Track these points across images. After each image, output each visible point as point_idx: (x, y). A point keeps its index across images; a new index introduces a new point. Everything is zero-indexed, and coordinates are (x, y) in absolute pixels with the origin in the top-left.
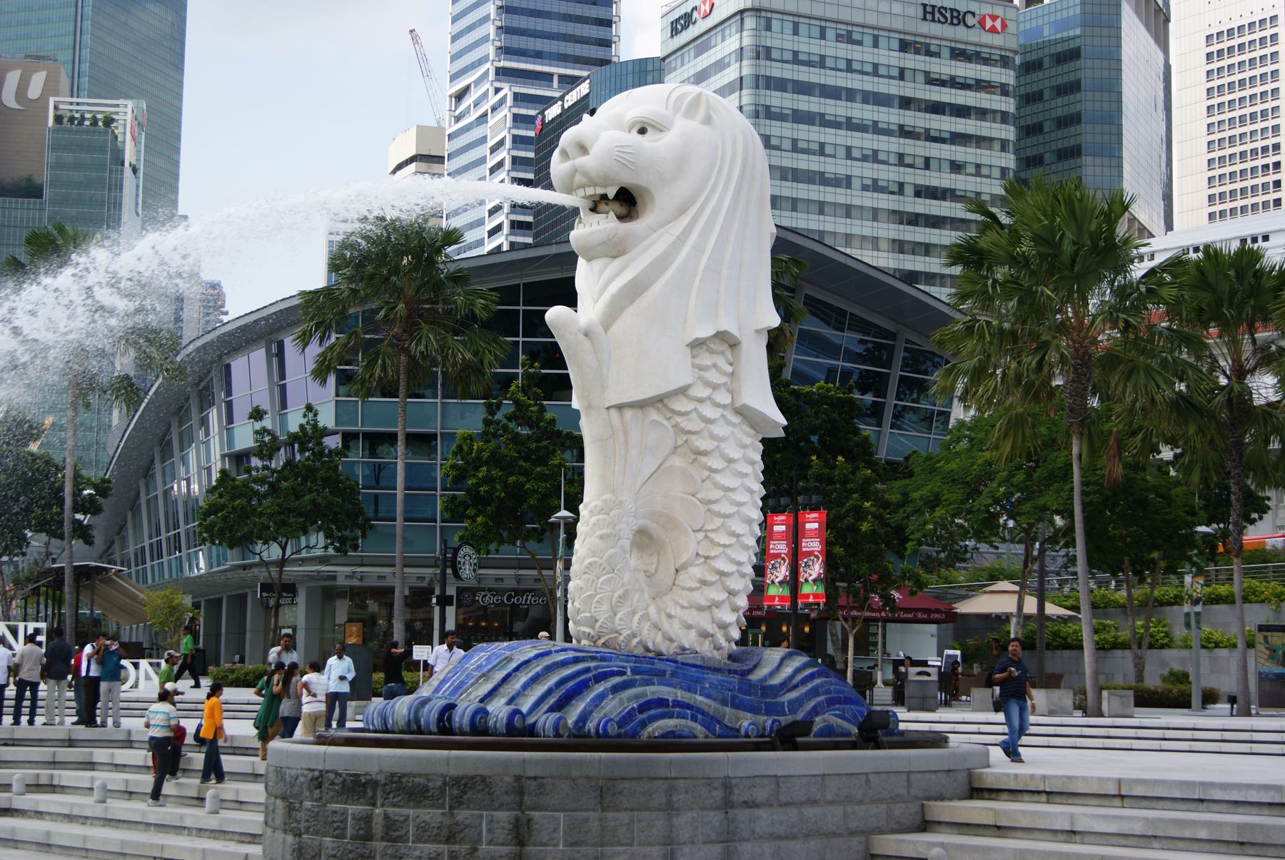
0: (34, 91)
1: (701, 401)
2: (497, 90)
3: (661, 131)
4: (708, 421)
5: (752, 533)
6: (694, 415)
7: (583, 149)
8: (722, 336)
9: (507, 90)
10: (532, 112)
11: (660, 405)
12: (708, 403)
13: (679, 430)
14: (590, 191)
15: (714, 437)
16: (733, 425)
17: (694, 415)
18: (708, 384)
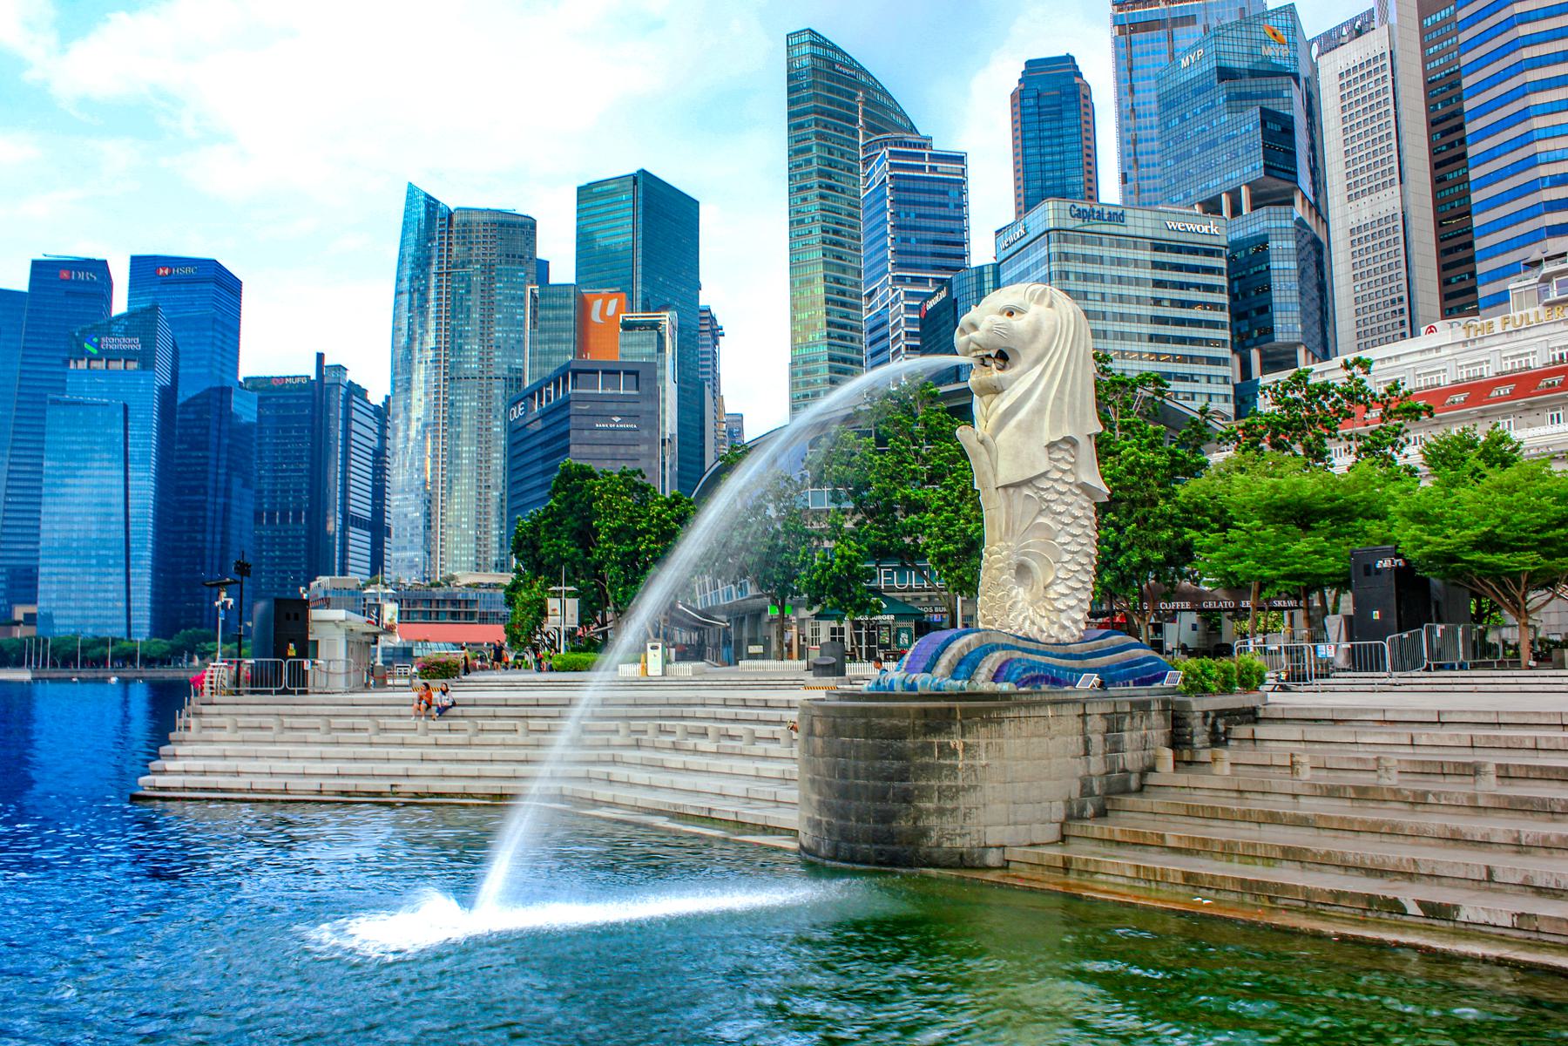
0: (610, 311)
1: (1056, 480)
2: (894, 291)
5: (1092, 563)
7: (974, 327)
8: (1066, 440)
9: (901, 290)
10: (918, 303)
14: (980, 353)
16: (1076, 495)
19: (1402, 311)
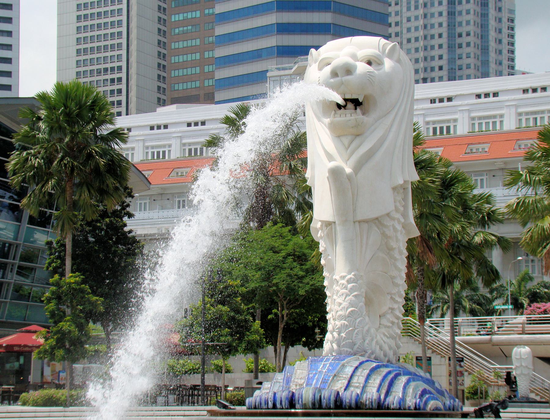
12: (396, 221)
13: (384, 234)
17: (392, 228)
19: (120, 80)
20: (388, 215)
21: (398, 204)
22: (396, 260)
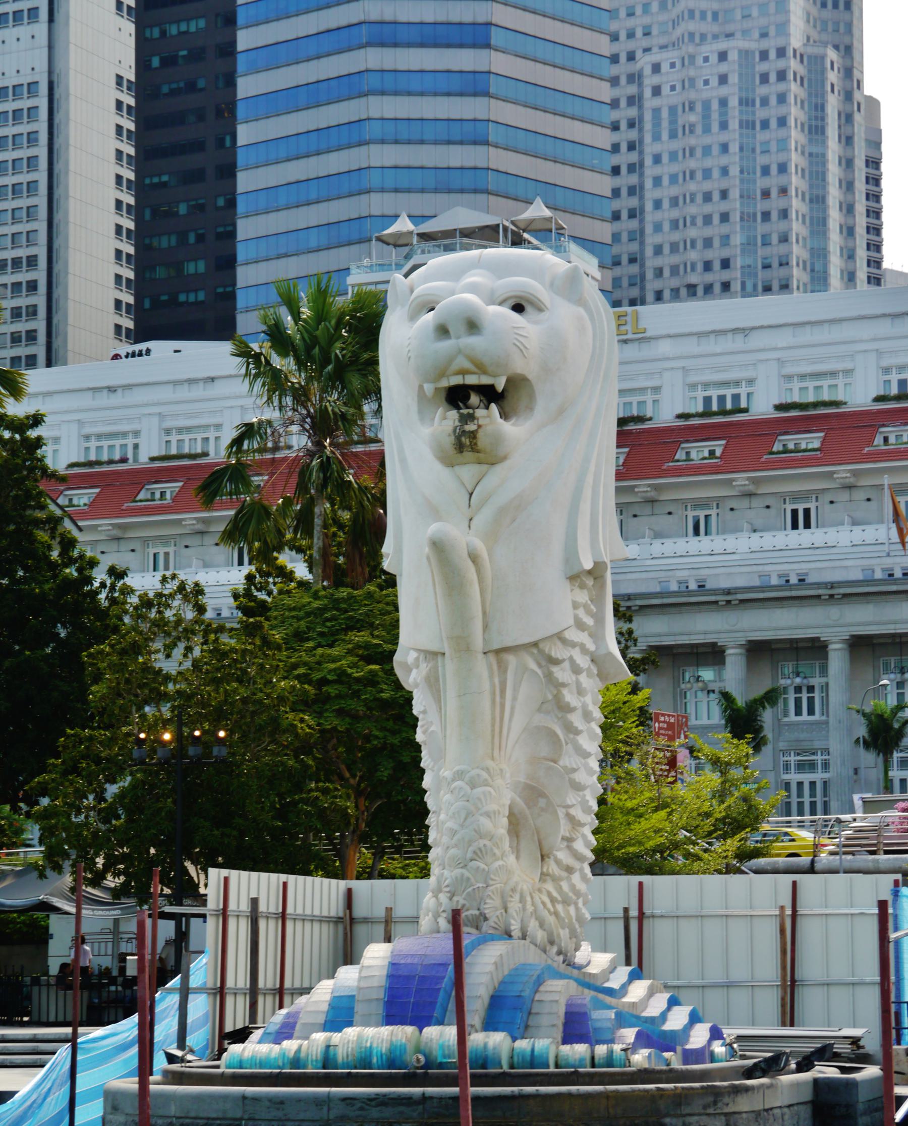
1: (573, 645)
3: (540, 310)
4: (576, 670)
6: (566, 665)
11: (535, 651)
12: (577, 649)
15: (580, 692)
17: (566, 665)
18: (580, 625)
20: (559, 637)
21: (581, 613)
22: (577, 732)
